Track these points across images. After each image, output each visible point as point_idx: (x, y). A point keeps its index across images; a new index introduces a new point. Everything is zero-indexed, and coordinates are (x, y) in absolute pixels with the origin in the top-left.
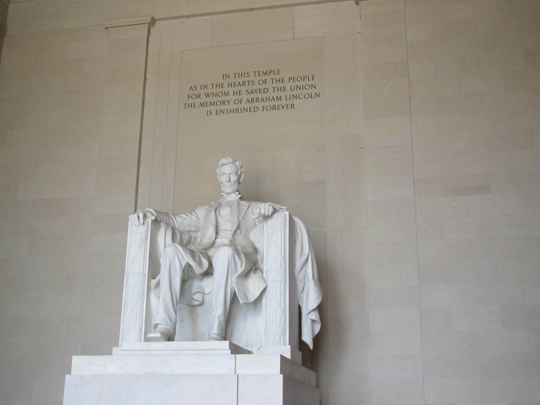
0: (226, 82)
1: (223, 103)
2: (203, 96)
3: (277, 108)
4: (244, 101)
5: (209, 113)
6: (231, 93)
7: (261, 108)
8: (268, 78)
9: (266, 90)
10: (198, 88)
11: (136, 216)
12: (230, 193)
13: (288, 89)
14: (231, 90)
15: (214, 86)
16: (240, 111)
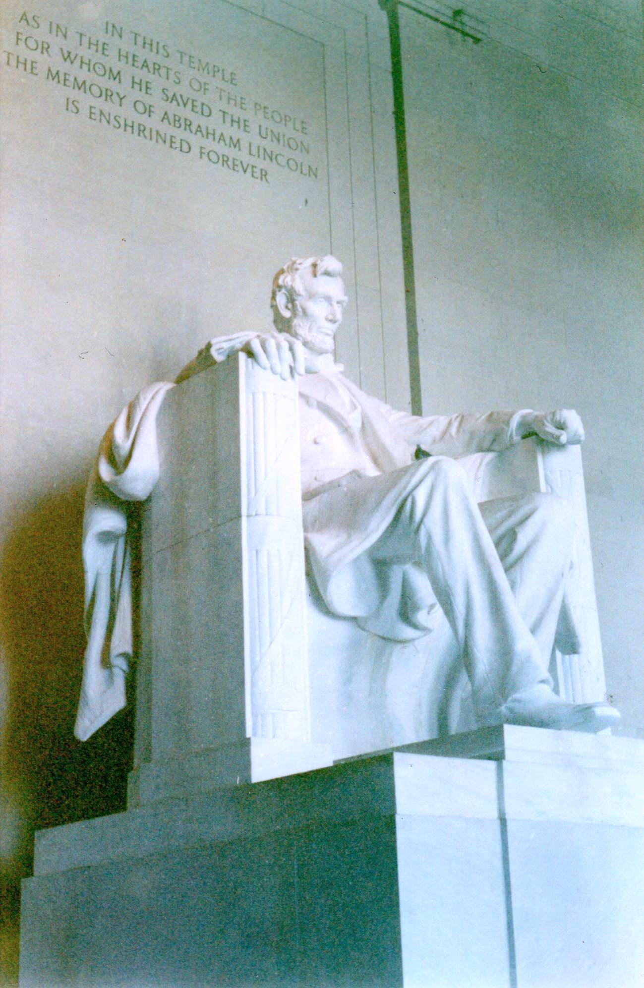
0: (114, 42)
1: (107, 94)
2: (54, 50)
3: (230, 163)
4: (158, 115)
5: (71, 105)
6: (126, 79)
7: (196, 150)
8: (215, 83)
9: (206, 112)
10: (44, 27)
11: (285, 346)
12: (321, 354)
13: (253, 128)
14: (128, 72)
15: (85, 41)
16: (147, 132)
